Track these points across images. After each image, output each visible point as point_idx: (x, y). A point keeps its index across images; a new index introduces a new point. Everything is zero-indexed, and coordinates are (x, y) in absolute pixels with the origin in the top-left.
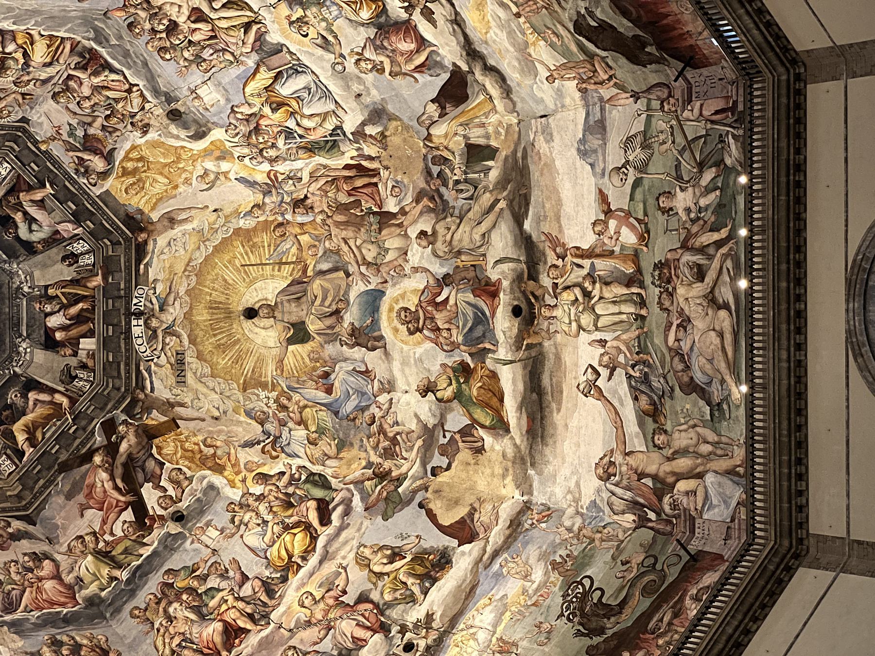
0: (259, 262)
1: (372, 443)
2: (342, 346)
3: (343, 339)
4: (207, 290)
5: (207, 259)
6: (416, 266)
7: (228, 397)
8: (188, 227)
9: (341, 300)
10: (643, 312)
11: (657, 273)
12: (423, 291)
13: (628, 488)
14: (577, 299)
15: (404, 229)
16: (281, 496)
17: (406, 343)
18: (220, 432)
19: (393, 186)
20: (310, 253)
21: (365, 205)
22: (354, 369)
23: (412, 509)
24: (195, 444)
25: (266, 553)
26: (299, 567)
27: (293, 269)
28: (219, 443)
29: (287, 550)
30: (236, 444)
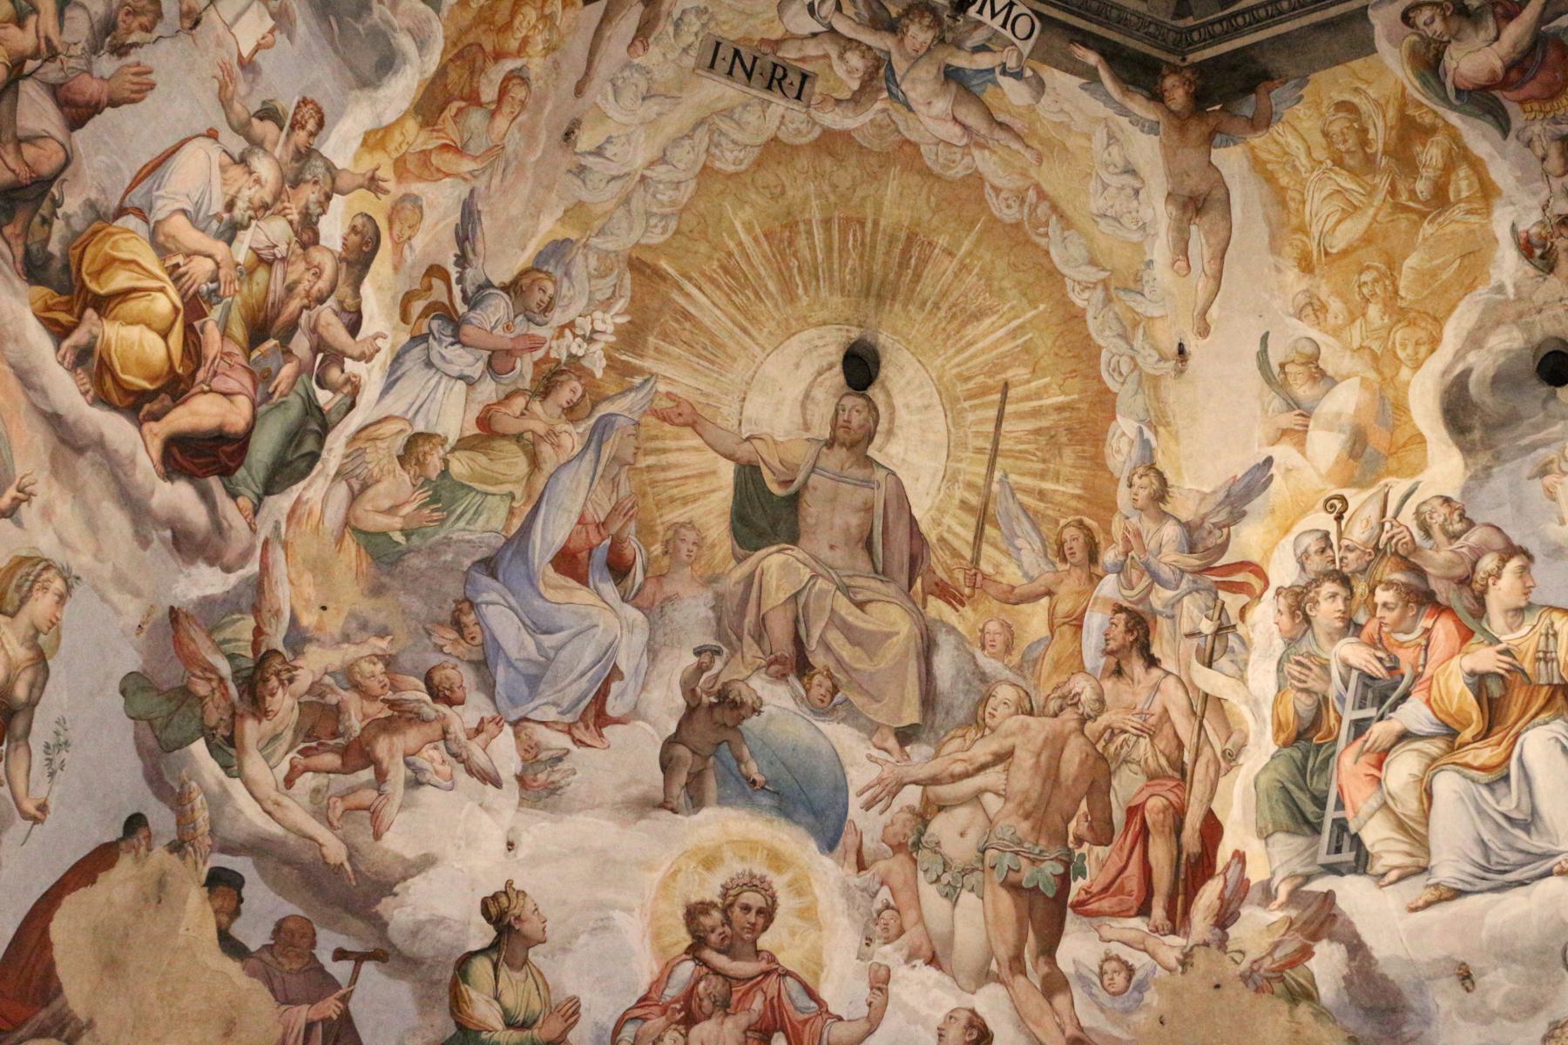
0: (1004, 445)
1: (367, 667)
2: (698, 652)
3: (718, 664)
4: (966, 245)
5: (1054, 275)
6: (893, 988)
7: (626, 201)
8: (1160, 250)
9: (835, 690)
12: (811, 994)
15: (1005, 973)
16: (294, 304)
17: (665, 886)
18: (530, 136)
19: (1130, 971)
20: (993, 626)
21: (1093, 855)
22: (615, 674)
23: (134, 793)
24: (525, 42)
25: (140, 213)
26: (60, 332)
27: (956, 554)
28: (501, 123)
29: (125, 294)
30: (480, 184)
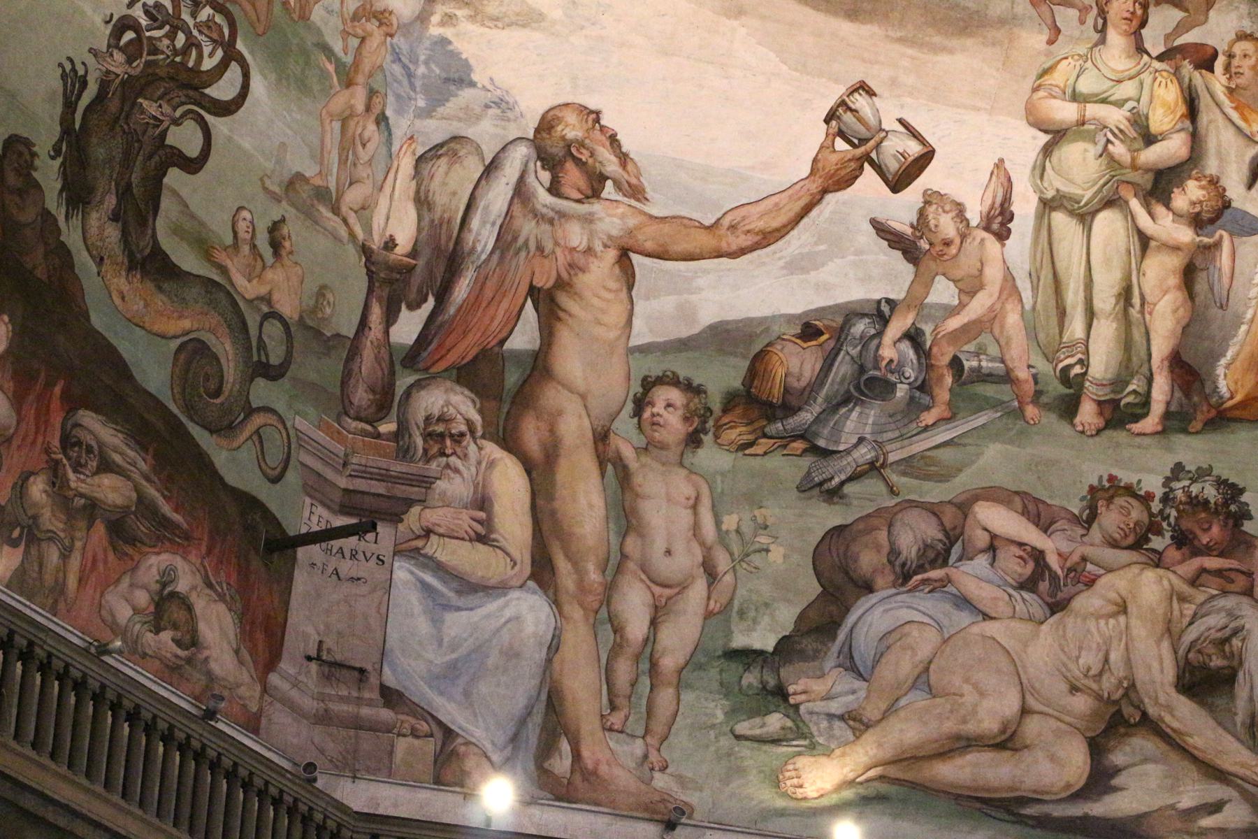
10: (1087, 413)
11: (1210, 493)
13: (506, 240)
14: (1150, 139)
